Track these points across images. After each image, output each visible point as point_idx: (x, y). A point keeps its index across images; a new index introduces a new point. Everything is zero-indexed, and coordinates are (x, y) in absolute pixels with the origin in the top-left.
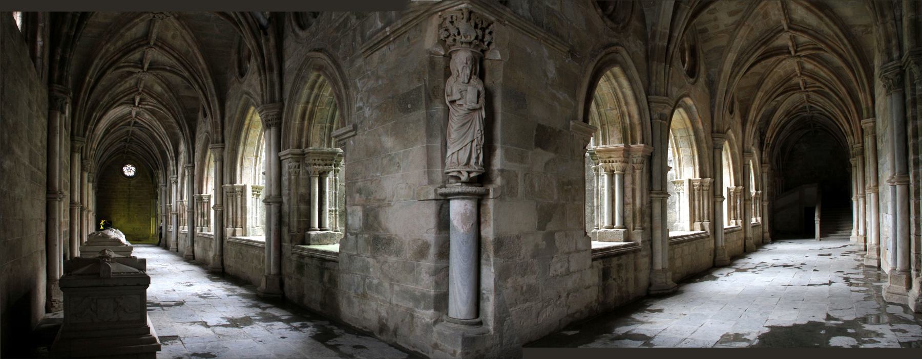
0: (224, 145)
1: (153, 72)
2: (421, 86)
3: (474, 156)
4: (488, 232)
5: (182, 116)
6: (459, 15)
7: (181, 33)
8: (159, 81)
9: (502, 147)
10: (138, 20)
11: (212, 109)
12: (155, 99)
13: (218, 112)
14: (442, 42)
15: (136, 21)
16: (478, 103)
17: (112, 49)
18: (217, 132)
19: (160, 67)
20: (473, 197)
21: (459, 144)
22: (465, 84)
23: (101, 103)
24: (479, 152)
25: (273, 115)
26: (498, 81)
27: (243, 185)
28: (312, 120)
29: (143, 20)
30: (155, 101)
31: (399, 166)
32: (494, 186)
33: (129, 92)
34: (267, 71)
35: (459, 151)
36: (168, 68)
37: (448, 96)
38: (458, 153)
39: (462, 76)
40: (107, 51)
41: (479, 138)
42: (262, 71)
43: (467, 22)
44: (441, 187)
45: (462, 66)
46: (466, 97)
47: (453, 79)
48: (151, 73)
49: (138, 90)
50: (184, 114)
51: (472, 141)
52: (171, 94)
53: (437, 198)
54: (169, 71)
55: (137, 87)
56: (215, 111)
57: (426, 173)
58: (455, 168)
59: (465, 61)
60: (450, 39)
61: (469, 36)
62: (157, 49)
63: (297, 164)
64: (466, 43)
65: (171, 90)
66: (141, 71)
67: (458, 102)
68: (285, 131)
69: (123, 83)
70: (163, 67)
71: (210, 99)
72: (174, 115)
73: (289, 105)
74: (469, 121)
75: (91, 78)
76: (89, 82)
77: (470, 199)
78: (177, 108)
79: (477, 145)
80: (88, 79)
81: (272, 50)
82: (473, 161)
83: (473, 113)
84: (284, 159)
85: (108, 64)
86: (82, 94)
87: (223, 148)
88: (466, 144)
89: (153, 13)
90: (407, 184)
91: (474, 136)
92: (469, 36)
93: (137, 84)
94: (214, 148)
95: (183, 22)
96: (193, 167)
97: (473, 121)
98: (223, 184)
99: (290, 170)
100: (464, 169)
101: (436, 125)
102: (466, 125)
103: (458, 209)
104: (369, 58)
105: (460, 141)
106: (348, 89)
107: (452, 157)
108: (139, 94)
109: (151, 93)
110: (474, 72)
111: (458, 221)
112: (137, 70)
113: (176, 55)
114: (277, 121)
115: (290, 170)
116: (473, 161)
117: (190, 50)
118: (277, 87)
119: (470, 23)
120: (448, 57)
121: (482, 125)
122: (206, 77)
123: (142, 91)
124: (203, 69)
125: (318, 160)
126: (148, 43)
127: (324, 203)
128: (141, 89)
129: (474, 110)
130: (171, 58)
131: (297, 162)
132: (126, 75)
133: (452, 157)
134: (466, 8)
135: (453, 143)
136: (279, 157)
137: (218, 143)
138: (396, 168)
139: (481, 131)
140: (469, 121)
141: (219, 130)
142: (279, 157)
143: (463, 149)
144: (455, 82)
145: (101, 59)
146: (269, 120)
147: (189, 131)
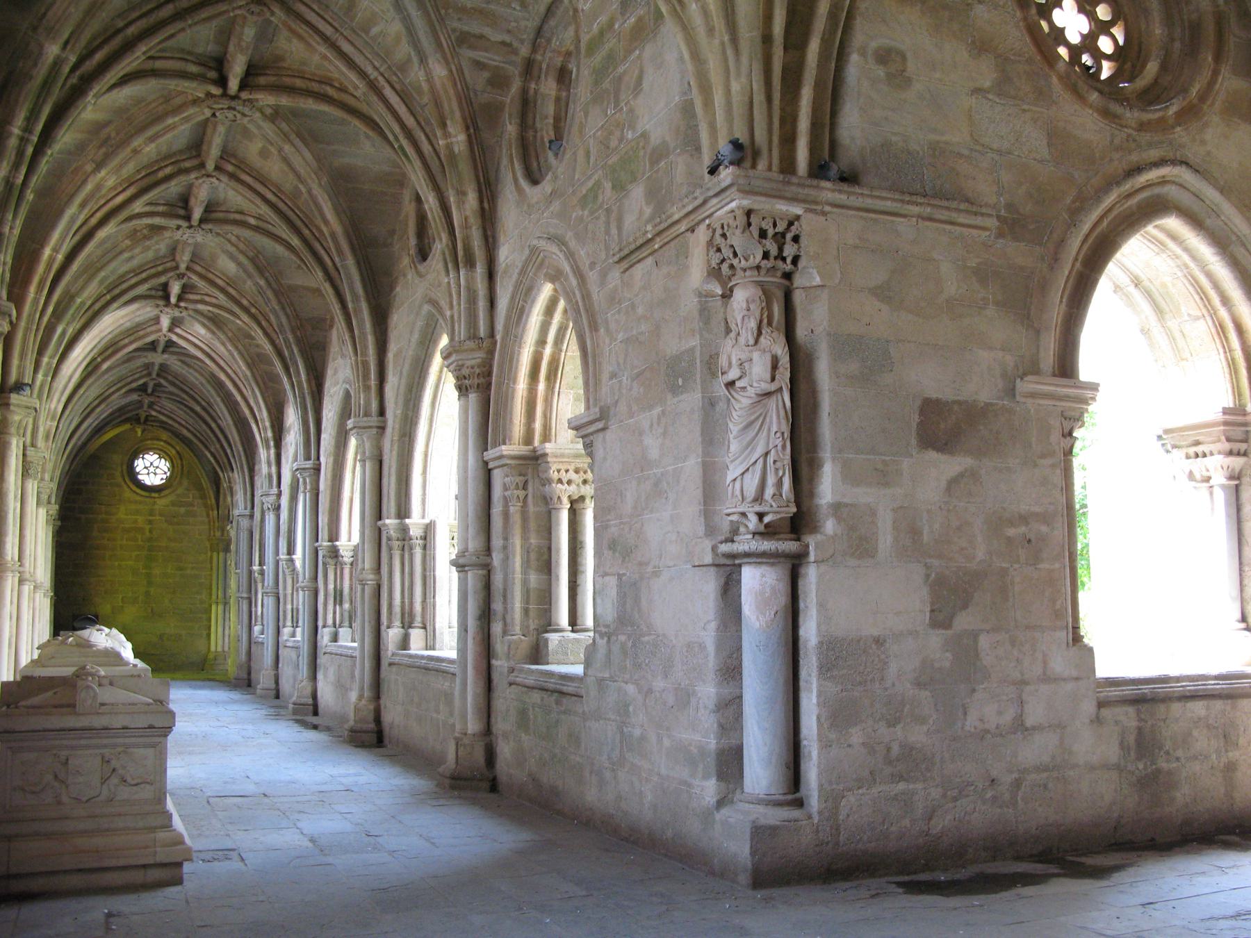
0: (385, 422)
1: (217, 229)
2: (694, 347)
3: (771, 480)
4: (810, 631)
5: (290, 337)
6: (733, 224)
7: (280, 150)
8: (232, 249)
9: (834, 459)
11: (356, 332)
12: (222, 290)
13: (370, 339)
14: (714, 273)
16: (773, 379)
17: (111, 182)
18: (367, 388)
19: (232, 216)
20: (776, 561)
21: (742, 463)
22: (750, 348)
23: (79, 300)
24: (781, 473)
25: (472, 368)
26: (821, 328)
27: (427, 521)
28: (555, 382)
31: (666, 498)
32: (819, 537)
33: (153, 271)
34: (461, 265)
35: (743, 474)
36: (252, 221)
37: (722, 374)
38: (742, 479)
39: (744, 331)
41: (779, 447)
42: (450, 265)
43: (743, 232)
44: (726, 541)
45: (741, 317)
46: (750, 373)
47: (730, 341)
48: (211, 230)
49: (177, 268)
50: (293, 332)
51: (767, 454)
52: (262, 282)
53: (716, 562)
54: (256, 229)
55: (174, 260)
56: (363, 334)
57: (702, 513)
58: (736, 507)
59: (744, 306)
60: (725, 267)
61: (752, 257)
62: (225, 179)
63: (520, 480)
64: (751, 268)
65: (261, 271)
66: (184, 224)
67: (738, 384)
69: (137, 251)
70: (238, 217)
71: (350, 306)
72: (270, 331)
73: (504, 346)
74: (758, 418)
75: (56, 250)
76: (52, 260)
77: (772, 564)
78: (277, 317)
79: (775, 462)
80: (47, 252)
81: (472, 220)
82: (770, 491)
85: (99, 215)
86: (32, 289)
87: (382, 428)
88: (753, 460)
90: (678, 532)
91: (768, 444)
92: (752, 257)
93: (173, 250)
94: (360, 428)
95: (284, 125)
96: (317, 469)
97: (765, 418)
99: (506, 494)
100: (750, 509)
101: (720, 421)
102: (753, 426)
103: (752, 579)
104: (627, 273)
105: (743, 456)
106: (596, 330)
108: (180, 276)
109: (210, 276)
110: (765, 321)
111: (750, 605)
112: (174, 223)
113: (270, 196)
114: (482, 380)
115: (506, 494)
116: (770, 491)
117: (304, 190)
118: (482, 304)
119: (750, 232)
120: (727, 296)
121: (784, 422)
122: (340, 252)
123: (188, 268)
124: (333, 235)
125: (567, 471)
126: (202, 165)
127: (581, 568)
128: (183, 266)
129: (768, 394)
130: (259, 201)
131: (520, 475)
132: (145, 231)
134: (738, 208)
136: (486, 463)
138: (664, 500)
139: (783, 433)
140: (758, 418)
141: (373, 382)
142: (486, 463)
146: (465, 378)
147: (308, 374)
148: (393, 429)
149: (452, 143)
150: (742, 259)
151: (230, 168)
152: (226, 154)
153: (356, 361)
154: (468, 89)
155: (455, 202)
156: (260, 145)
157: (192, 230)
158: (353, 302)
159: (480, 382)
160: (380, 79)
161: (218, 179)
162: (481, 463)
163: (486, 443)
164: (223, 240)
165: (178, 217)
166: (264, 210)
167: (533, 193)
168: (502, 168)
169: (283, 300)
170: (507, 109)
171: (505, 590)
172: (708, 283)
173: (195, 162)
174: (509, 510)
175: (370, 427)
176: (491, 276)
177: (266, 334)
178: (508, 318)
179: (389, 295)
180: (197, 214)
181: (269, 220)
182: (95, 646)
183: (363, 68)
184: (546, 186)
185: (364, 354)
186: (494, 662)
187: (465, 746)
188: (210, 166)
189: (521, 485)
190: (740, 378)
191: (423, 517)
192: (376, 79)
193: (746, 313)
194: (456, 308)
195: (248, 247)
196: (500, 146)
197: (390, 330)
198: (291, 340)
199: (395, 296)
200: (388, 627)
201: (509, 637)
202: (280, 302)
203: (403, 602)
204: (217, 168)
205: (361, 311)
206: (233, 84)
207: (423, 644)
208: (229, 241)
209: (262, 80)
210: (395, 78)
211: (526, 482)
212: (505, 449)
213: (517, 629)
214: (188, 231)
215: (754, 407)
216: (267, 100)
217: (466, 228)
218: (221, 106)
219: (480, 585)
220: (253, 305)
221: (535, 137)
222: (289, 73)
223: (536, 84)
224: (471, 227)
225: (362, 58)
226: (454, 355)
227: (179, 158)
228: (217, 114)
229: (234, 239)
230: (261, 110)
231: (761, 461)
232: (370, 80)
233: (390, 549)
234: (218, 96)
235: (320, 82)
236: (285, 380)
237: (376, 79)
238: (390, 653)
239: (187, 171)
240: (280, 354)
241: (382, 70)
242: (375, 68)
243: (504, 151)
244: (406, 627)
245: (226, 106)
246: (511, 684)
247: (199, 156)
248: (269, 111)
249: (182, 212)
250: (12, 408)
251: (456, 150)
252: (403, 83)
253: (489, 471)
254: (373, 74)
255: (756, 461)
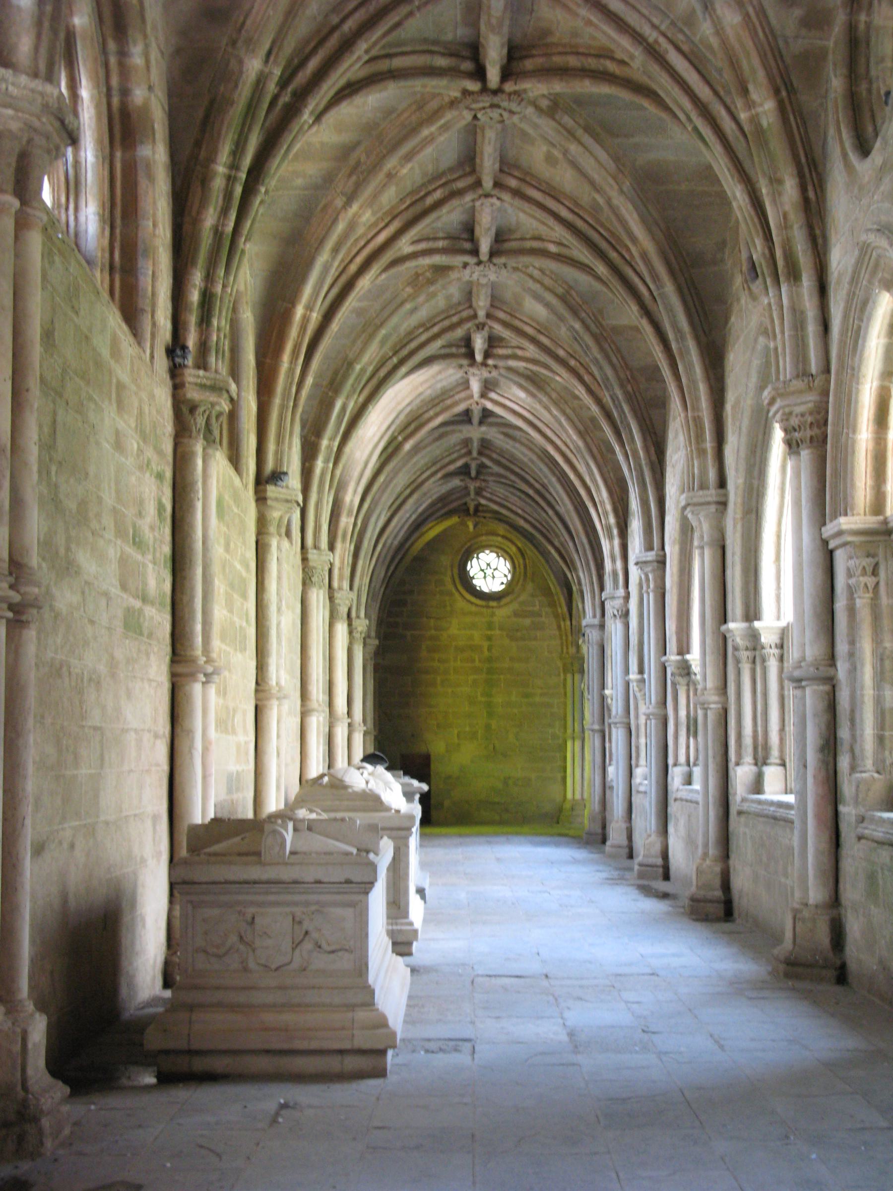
0: (726, 495)
1: (512, 262)
5: (619, 393)
7: (565, 153)
8: (536, 287)
10: (433, 129)
11: (684, 380)
12: (533, 340)
13: (702, 388)
15: (425, 132)
17: (367, 217)
18: (702, 452)
23: (358, 367)
25: (803, 415)
29: (445, 128)
30: (531, 351)
33: (447, 323)
36: (553, 248)
40: (352, 226)
48: (505, 265)
49: (475, 316)
50: (622, 386)
52: (577, 326)
54: (558, 257)
55: (471, 307)
56: (693, 382)
62: (507, 197)
63: (868, 562)
65: (575, 313)
66: (472, 260)
68: (835, 459)
69: (421, 299)
70: (536, 244)
71: (674, 346)
72: (594, 387)
75: (309, 308)
76: (305, 320)
78: (601, 368)
80: (299, 311)
81: (792, 216)
84: (837, 548)
85: (359, 260)
86: (286, 357)
87: (723, 504)
89: (471, 109)
93: (469, 295)
94: (695, 505)
95: (567, 120)
96: (662, 562)
98: (725, 621)
108: (480, 327)
109: (517, 323)
112: (459, 260)
113: (564, 213)
114: (816, 431)
115: (850, 582)
117: (601, 201)
118: (812, 329)
122: (655, 277)
123: (489, 316)
124: (644, 256)
126: (478, 184)
128: (481, 314)
130: (551, 221)
131: (868, 556)
132: (428, 274)
136: (825, 542)
137: (708, 488)
141: (709, 444)
145: (336, 250)
147: (645, 440)
148: (735, 504)
149: (757, 115)
151: (513, 183)
152: (506, 165)
153: (687, 416)
154: (775, 37)
155: (768, 194)
156: (544, 148)
157: (481, 267)
158: (677, 341)
159: (813, 434)
160: (662, 40)
161: (498, 199)
162: (818, 542)
163: (824, 515)
164: (522, 276)
165: (463, 252)
166: (559, 232)
167: (865, 168)
168: (830, 140)
169: (606, 346)
170: (830, 57)
171: (853, 711)
173: (470, 180)
174: (855, 604)
175: (708, 503)
176: (822, 289)
177: (590, 391)
178: (842, 343)
179: (725, 328)
180: (485, 246)
181: (566, 242)
182: (351, 787)
183: (638, 29)
184: (877, 157)
185: (696, 408)
186: (842, 809)
187: (803, 920)
188: (488, 183)
189: (869, 570)
191: (778, 618)
192: (656, 41)
194: (779, 336)
195: (556, 281)
196: (826, 110)
197: (726, 374)
198: (620, 397)
199: (730, 329)
200: (737, 764)
201: (858, 775)
202: (602, 349)
203: (755, 732)
204: (497, 185)
205: (688, 352)
206: (493, 75)
207: (780, 786)
208: (531, 277)
209: (529, 64)
210: (680, 37)
211: (876, 565)
212: (845, 522)
213: (869, 763)
214: (477, 268)
216: (536, 88)
217: (786, 228)
218: (481, 105)
219: (822, 705)
220: (571, 356)
221: (869, 91)
222: (560, 49)
223: (868, 14)
224: (791, 227)
225: (636, 16)
226: (779, 400)
227: (449, 177)
228: (479, 116)
229: (536, 273)
230: (534, 104)
232: (648, 44)
233: (738, 661)
234: (477, 93)
235: (598, 56)
236: (617, 449)
237: (656, 41)
238: (738, 798)
239: (460, 193)
240: (609, 416)
241: (663, 28)
242: (654, 27)
243: (831, 116)
244: (759, 764)
245: (487, 104)
246: (860, 838)
247: (473, 171)
248: (544, 103)
249: (467, 246)
250: (269, 502)
251: (765, 123)
252: (693, 42)
253: (831, 553)
254: (652, 35)
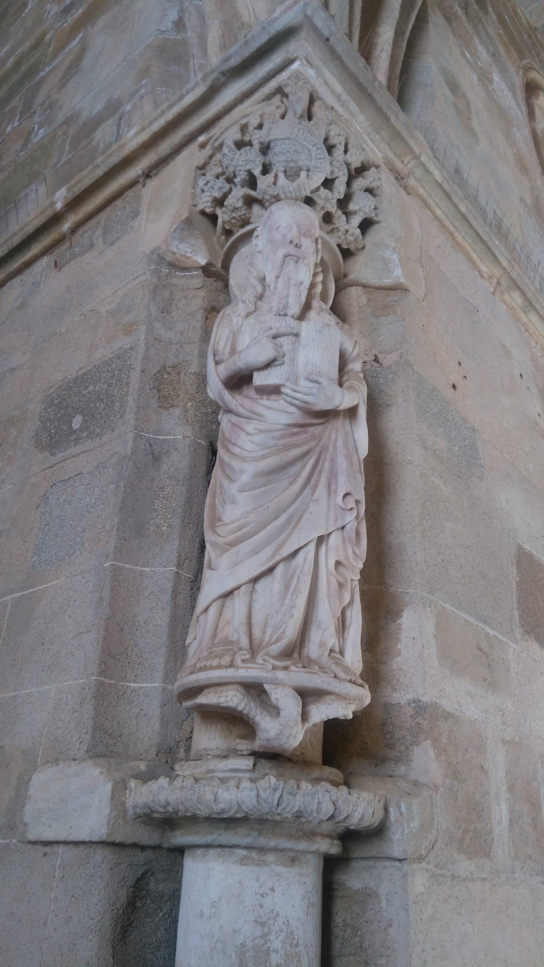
21: (256, 551)
35: (255, 580)
46: (293, 360)
51: (321, 540)
53: (118, 839)
58: (231, 665)
67: (259, 379)
83: (319, 429)
100: (280, 675)
101: (167, 490)
102: (293, 470)
107: (220, 613)
133: (220, 613)
135: (232, 544)
139: (357, 502)
143: (279, 570)
144: (248, 315)
150: (281, 176)
172: (182, 240)
190: (268, 365)
193: (291, 250)
215: (294, 434)
231: (312, 548)
255: (296, 552)
